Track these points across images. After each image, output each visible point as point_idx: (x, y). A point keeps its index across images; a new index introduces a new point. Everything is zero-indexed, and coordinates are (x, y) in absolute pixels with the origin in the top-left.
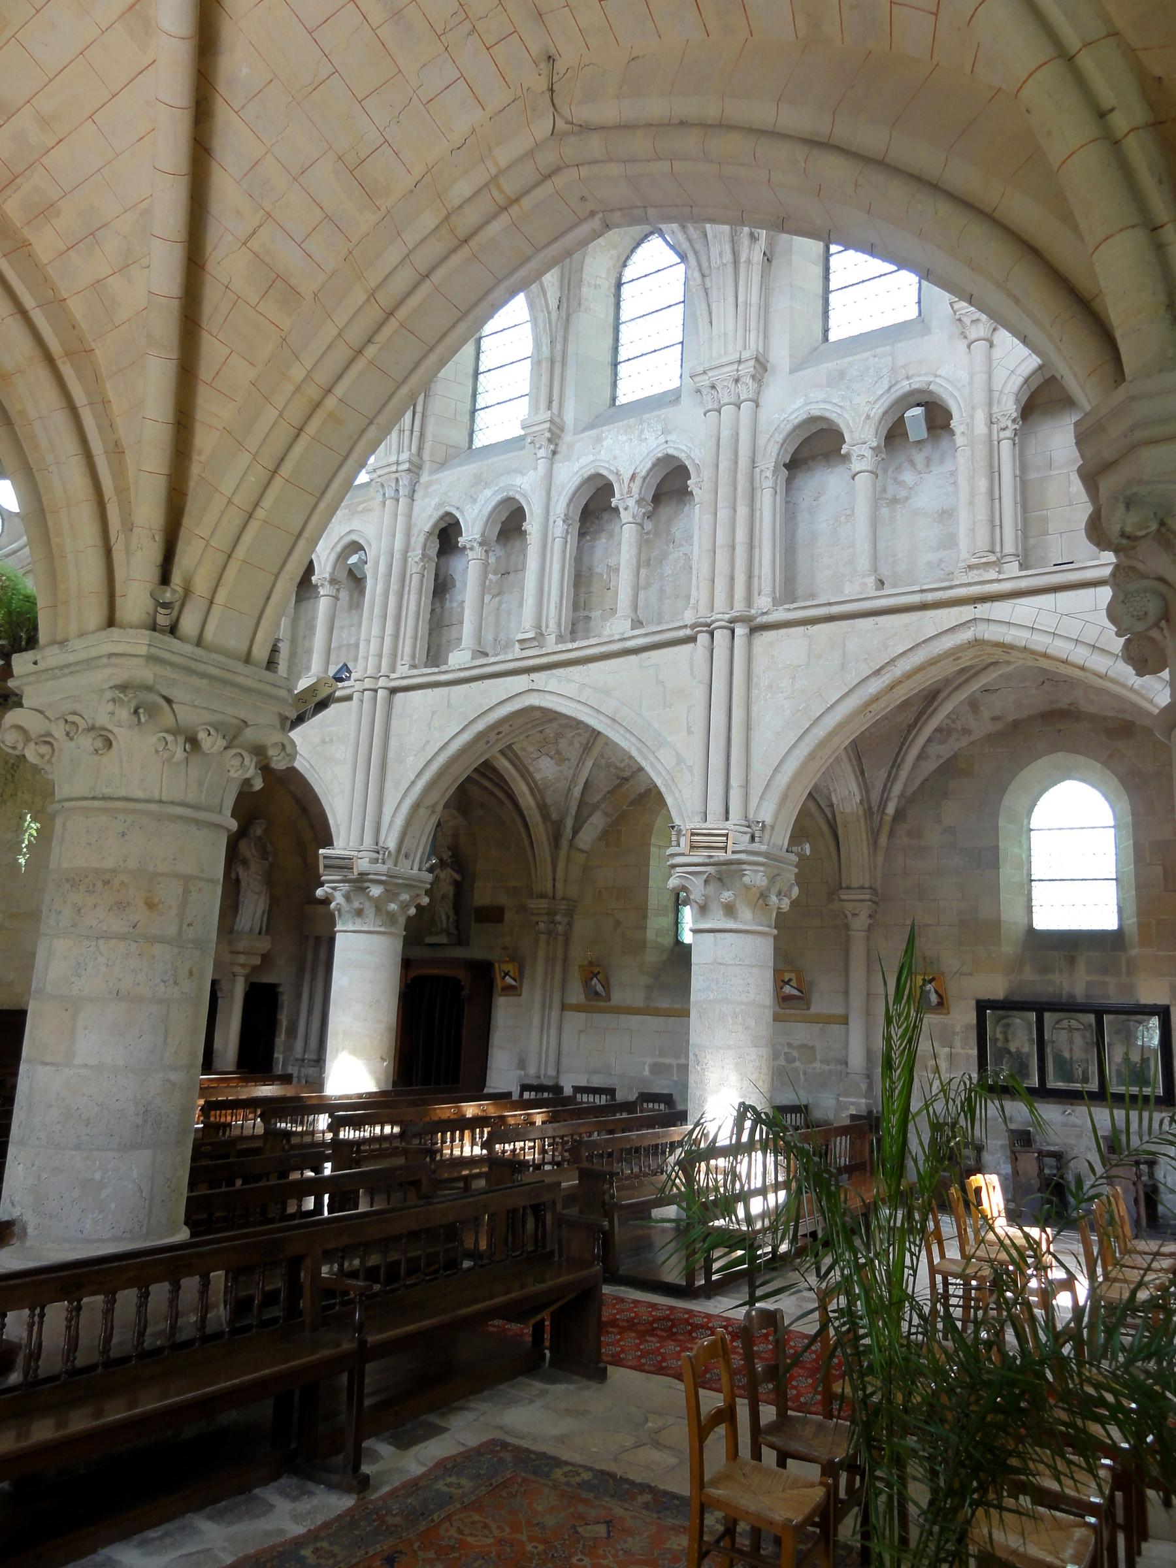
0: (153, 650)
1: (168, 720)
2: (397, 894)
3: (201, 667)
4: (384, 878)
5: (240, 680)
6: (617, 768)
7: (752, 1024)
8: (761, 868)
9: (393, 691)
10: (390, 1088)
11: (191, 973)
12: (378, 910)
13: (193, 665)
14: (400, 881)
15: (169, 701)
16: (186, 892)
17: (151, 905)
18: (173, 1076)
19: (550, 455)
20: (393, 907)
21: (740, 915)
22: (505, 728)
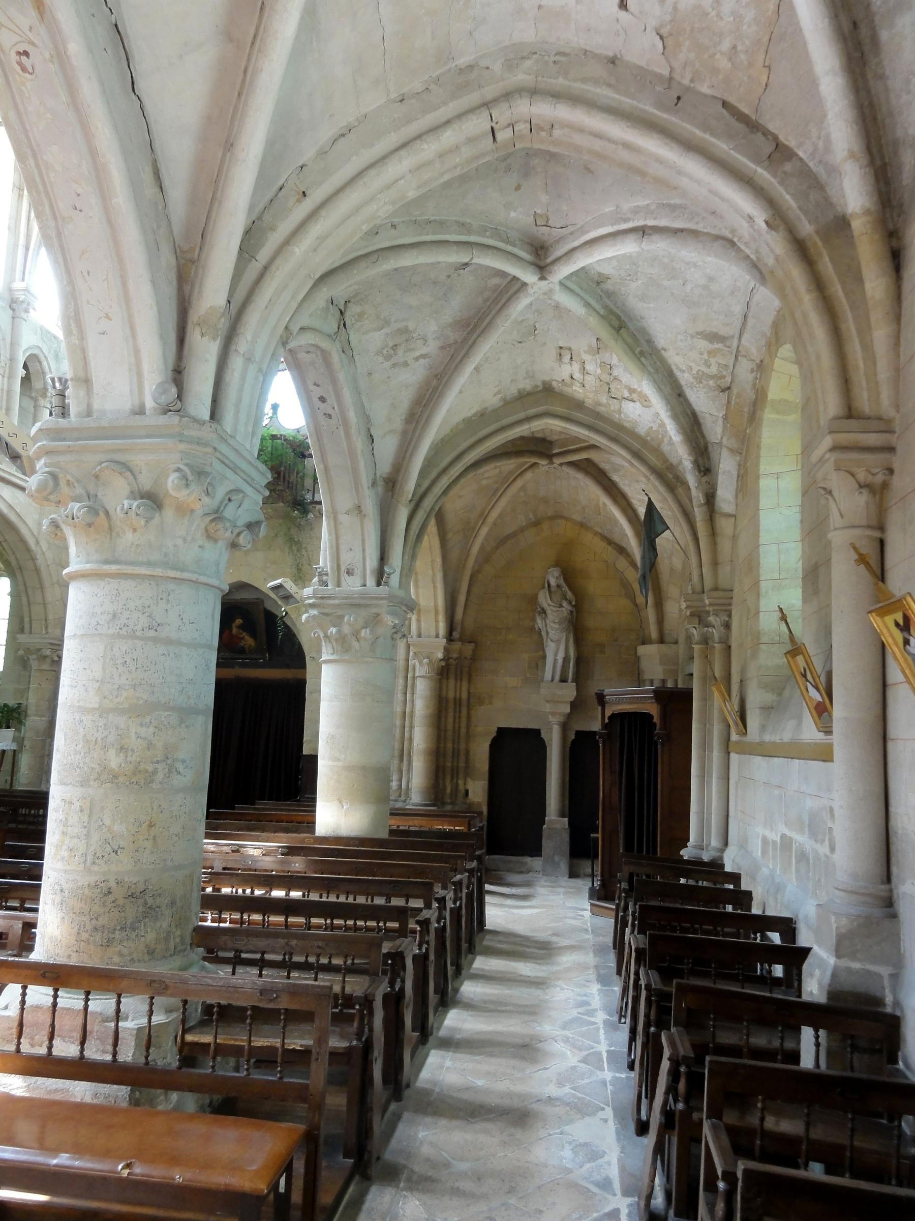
2: (342, 617)
4: (311, 601)
6: (712, 377)
14: (337, 602)
20: (334, 630)
22: (317, 392)
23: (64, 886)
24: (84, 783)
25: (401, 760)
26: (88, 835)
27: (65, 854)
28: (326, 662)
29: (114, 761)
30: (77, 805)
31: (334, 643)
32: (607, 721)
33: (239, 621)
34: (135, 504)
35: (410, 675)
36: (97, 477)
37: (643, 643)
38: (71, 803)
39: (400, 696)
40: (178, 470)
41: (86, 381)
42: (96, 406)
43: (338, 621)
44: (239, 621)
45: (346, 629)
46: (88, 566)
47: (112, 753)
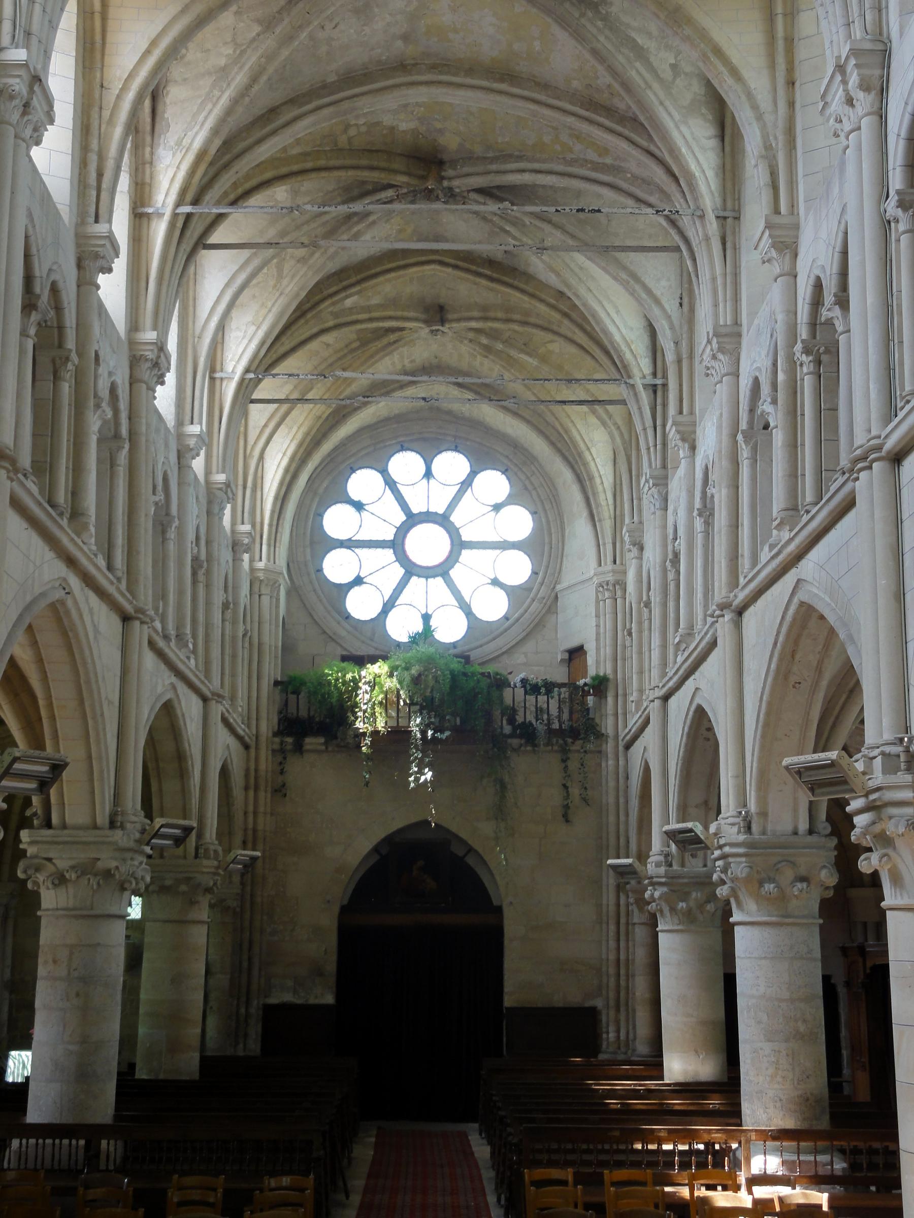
0: (33, 839)
1: (50, 868)
2: (688, 894)
3: (60, 839)
4: (663, 880)
5: (84, 839)
7: (765, 1018)
8: (744, 859)
9: (666, 698)
10: (726, 1080)
11: (78, 995)
12: (673, 910)
13: (55, 839)
14: (686, 881)
15: (49, 860)
16: (71, 953)
17: (55, 962)
18: (71, 1047)
19: (688, 453)
20: (682, 905)
21: (745, 907)
23: (782, 1097)
24: (769, 1041)
25: (618, 1010)
26: (793, 1069)
27: (779, 1079)
28: (662, 931)
29: (802, 1028)
30: (784, 1052)
31: (681, 916)
32: (868, 971)
33: (421, 863)
34: (805, 885)
35: (623, 920)
36: (777, 870)
37: (853, 886)
38: (779, 1051)
39: (612, 944)
40: (824, 867)
41: (763, 814)
42: (769, 828)
43: (685, 897)
44: (421, 863)
45: (692, 904)
46: (774, 919)
47: (800, 1023)
